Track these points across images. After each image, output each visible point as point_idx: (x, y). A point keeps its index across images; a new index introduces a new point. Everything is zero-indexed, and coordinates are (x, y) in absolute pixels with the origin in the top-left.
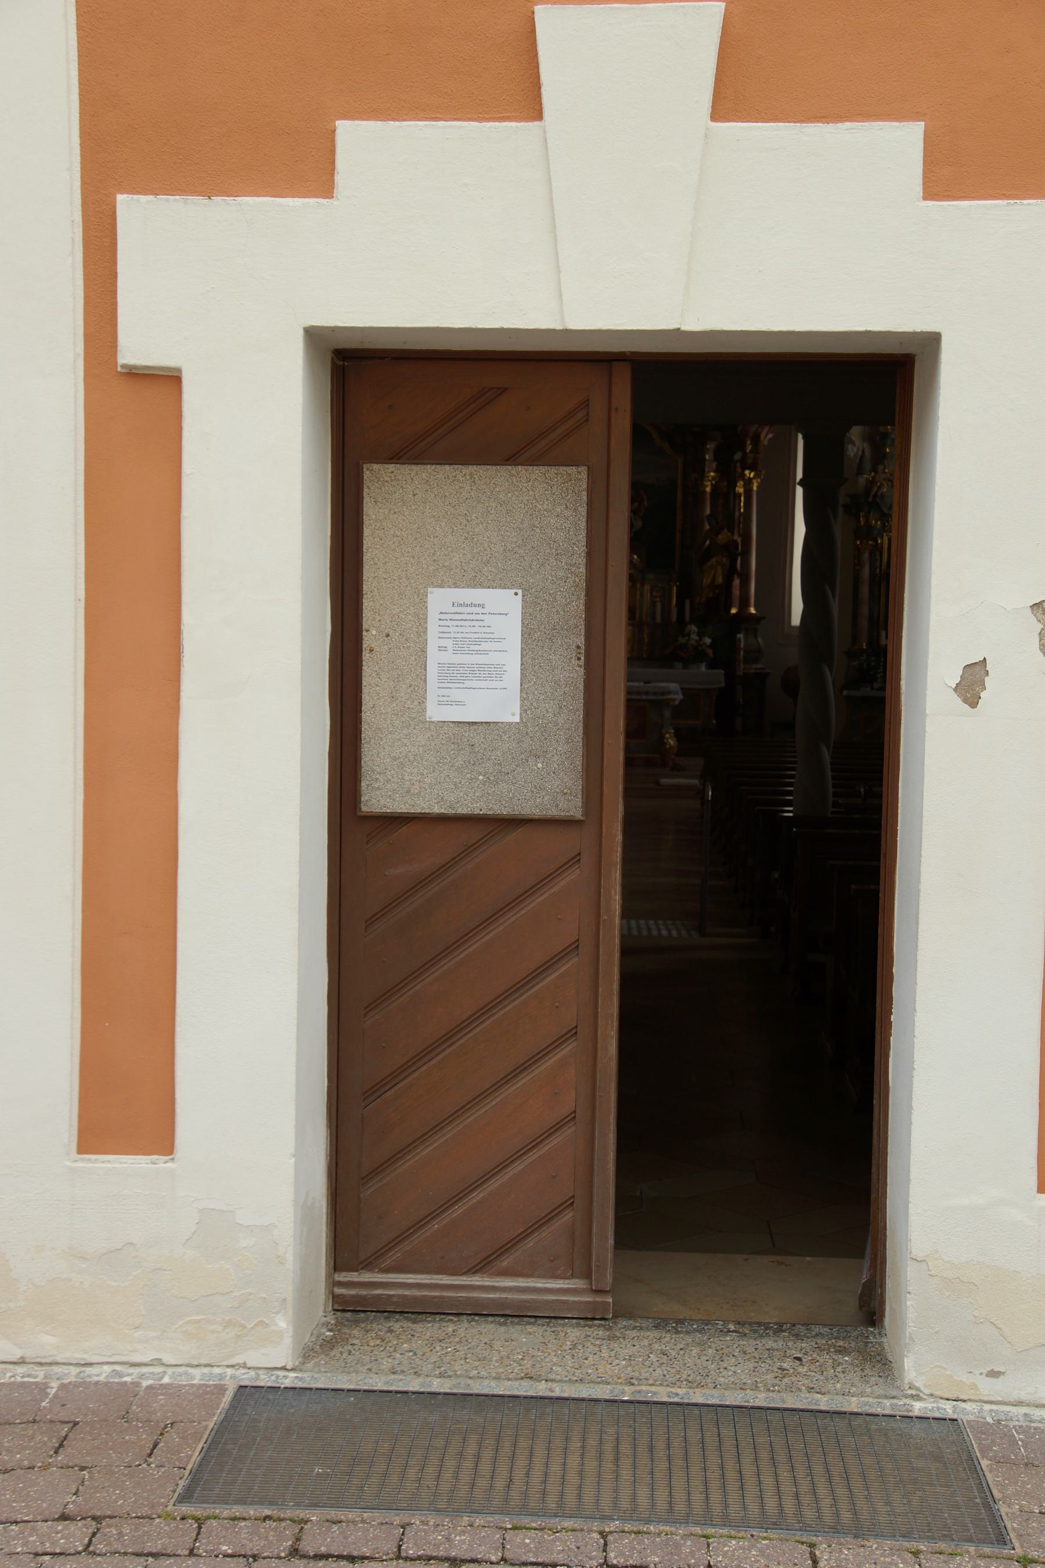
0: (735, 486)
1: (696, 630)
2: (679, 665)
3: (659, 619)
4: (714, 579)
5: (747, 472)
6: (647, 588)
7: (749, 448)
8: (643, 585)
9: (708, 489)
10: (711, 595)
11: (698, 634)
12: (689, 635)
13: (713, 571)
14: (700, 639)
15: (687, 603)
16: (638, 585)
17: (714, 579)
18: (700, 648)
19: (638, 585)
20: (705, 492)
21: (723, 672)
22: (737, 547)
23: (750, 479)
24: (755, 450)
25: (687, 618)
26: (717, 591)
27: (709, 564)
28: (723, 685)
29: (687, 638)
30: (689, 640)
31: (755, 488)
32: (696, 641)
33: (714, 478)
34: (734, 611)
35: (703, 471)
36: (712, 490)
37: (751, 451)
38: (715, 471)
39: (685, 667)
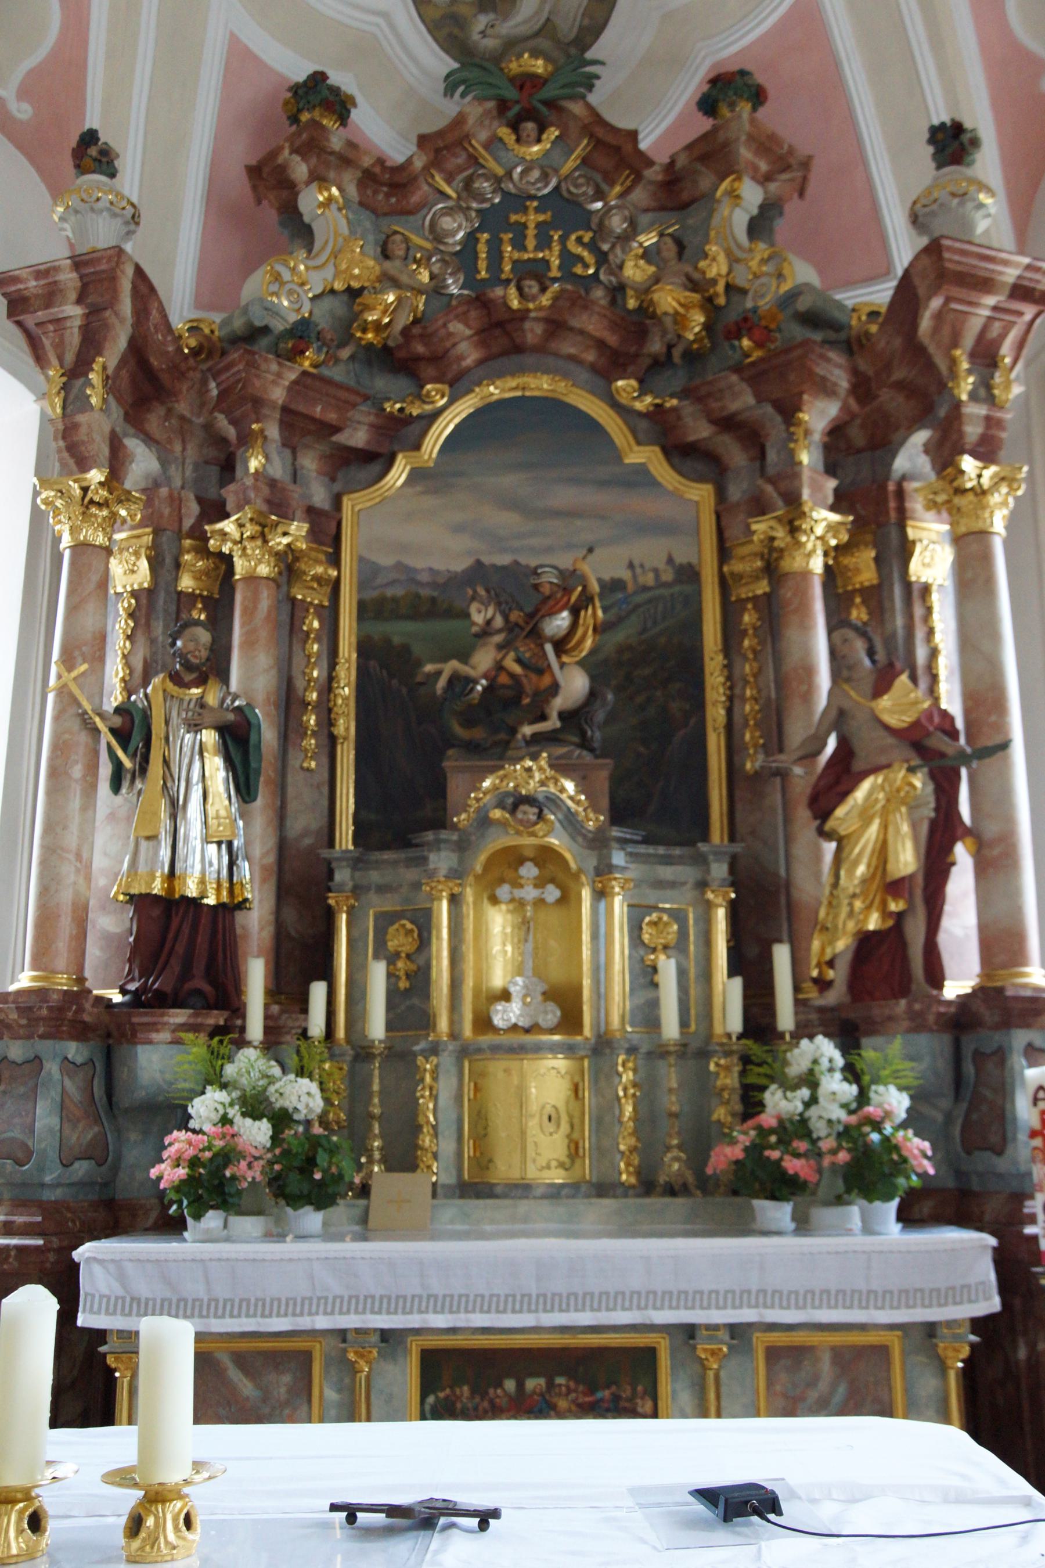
0: (906, 548)
1: (840, 1062)
2: (780, 1213)
3: (671, 1029)
4: (882, 853)
5: (968, 464)
6: (619, 904)
7: (966, 385)
8: (601, 894)
9: (817, 564)
10: (873, 923)
11: (852, 1073)
12: (811, 1080)
13: (874, 828)
14: (863, 1098)
15: (782, 955)
16: (586, 894)
17: (882, 853)
18: (875, 1137)
19: (586, 894)
20: (806, 574)
21: (993, 1241)
22: (954, 734)
23: (981, 492)
24: (985, 392)
25: (786, 1018)
26: (894, 906)
27: (860, 794)
28: (994, 1304)
29: (805, 1093)
30: (813, 1101)
31: (998, 523)
32: (844, 1106)
33: (831, 528)
34: (954, 989)
35: (793, 501)
36: (827, 567)
37: (973, 396)
38: (833, 508)
39: (803, 1225)
